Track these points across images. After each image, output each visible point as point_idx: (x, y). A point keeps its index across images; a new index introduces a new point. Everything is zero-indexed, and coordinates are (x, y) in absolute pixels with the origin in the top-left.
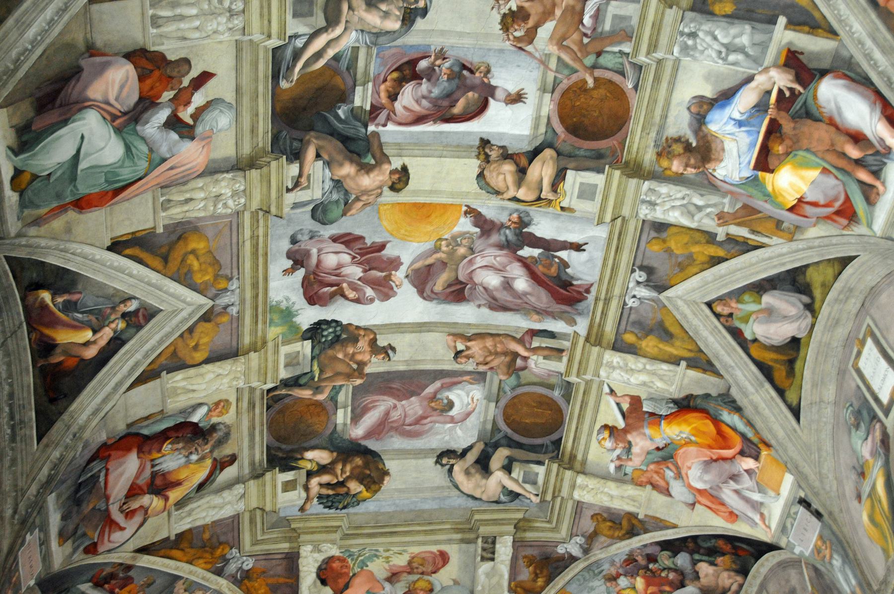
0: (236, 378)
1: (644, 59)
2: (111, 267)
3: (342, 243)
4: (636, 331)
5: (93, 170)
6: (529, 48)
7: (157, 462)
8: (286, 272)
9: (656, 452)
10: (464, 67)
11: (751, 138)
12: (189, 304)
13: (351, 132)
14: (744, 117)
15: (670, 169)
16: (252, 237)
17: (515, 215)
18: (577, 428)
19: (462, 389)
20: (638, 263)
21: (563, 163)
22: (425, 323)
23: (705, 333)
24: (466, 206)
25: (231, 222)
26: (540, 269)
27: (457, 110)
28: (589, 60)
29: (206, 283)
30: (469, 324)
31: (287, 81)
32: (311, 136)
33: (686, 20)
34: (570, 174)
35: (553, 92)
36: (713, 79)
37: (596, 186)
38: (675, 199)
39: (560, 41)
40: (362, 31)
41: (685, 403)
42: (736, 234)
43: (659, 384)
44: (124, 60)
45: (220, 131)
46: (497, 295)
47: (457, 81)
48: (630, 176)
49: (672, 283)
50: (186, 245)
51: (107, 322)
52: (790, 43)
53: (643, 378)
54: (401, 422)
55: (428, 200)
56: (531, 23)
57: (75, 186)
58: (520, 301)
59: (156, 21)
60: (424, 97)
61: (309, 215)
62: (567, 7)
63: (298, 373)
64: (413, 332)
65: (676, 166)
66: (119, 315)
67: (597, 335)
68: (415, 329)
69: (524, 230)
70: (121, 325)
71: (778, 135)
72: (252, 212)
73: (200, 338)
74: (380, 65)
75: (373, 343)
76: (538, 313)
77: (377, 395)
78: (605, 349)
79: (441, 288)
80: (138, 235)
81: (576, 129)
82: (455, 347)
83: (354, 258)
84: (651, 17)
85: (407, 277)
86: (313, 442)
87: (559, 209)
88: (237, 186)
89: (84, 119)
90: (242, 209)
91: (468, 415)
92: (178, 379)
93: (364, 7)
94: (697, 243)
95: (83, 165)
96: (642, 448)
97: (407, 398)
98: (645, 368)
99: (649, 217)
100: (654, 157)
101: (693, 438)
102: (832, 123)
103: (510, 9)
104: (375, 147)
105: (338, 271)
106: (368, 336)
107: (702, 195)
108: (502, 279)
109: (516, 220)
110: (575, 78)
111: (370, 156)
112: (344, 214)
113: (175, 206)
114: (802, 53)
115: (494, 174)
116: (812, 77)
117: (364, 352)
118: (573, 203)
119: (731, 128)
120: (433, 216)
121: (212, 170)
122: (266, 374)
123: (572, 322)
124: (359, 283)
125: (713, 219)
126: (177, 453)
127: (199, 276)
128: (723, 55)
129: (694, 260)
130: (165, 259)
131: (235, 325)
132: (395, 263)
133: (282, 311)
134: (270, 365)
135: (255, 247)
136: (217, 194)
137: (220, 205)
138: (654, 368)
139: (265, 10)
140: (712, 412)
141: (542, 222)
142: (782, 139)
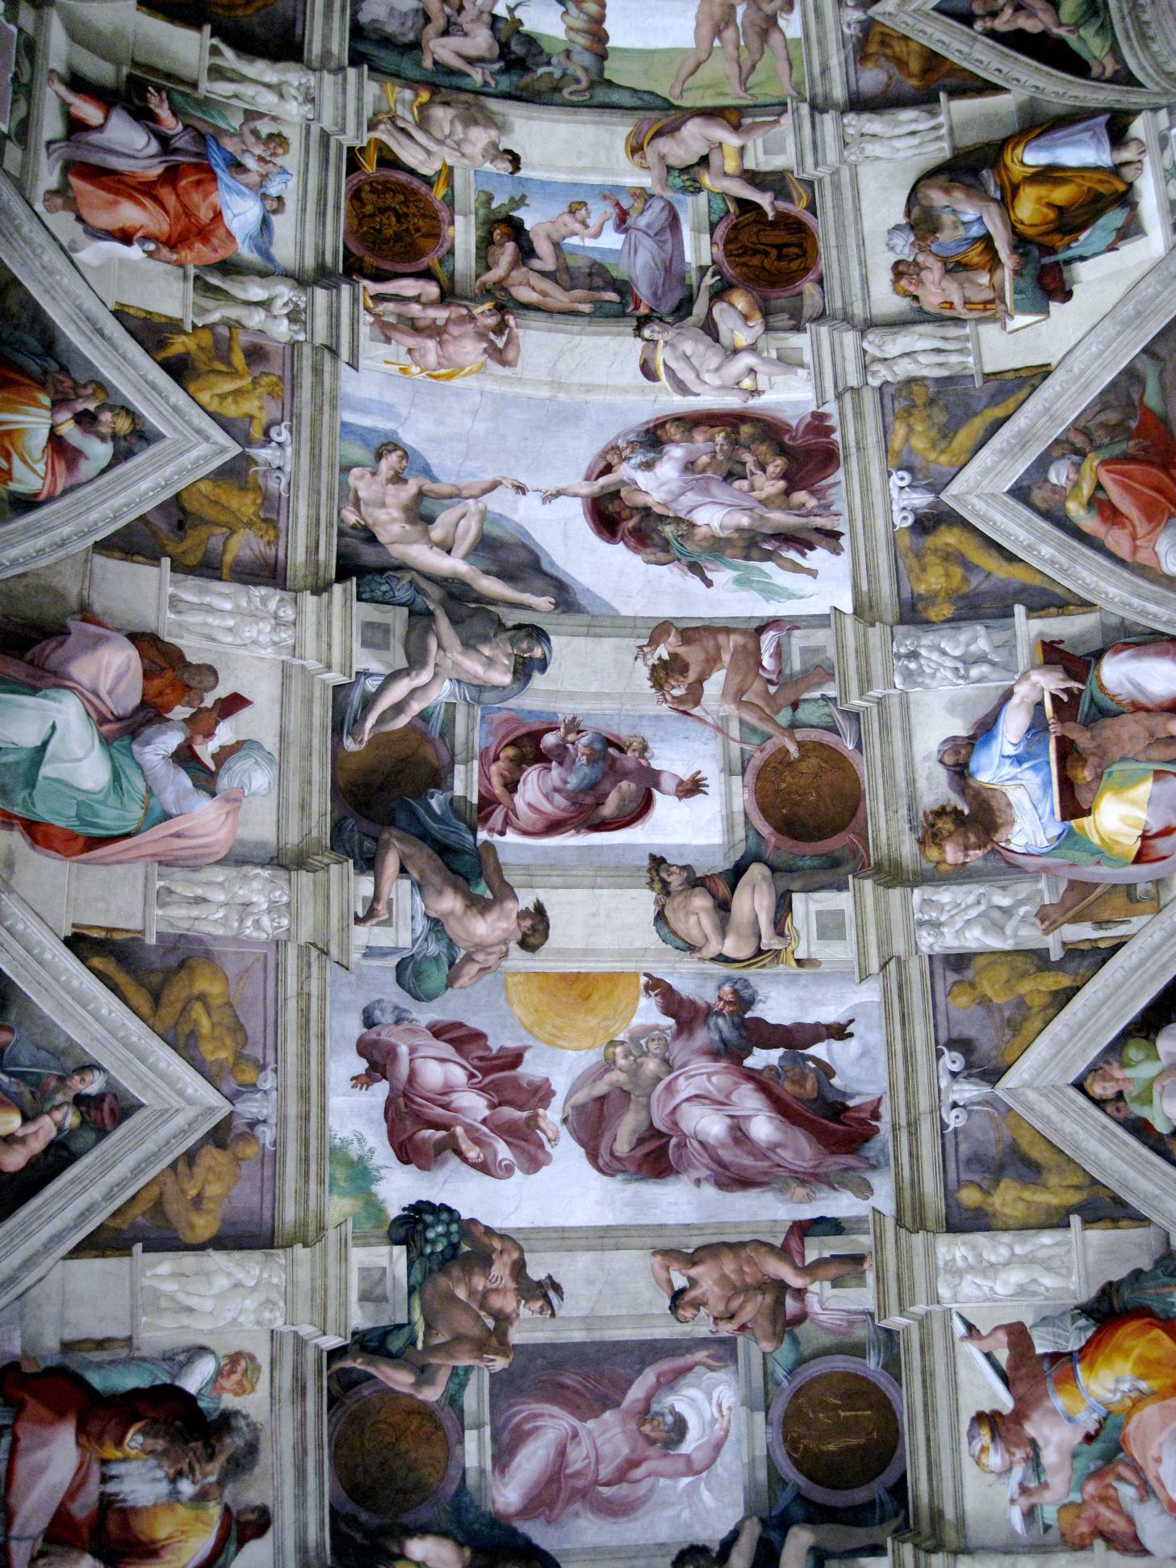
0: (268, 1303)
1: (858, 702)
2: (67, 987)
3: (446, 1041)
4: (976, 1178)
5: (62, 788)
6: (696, 711)
7: (115, 1469)
8: (357, 1081)
9: (1086, 1447)
10: (609, 743)
11: (1042, 774)
12: (190, 1101)
13: (452, 840)
14: (1021, 749)
15: (944, 861)
16: (299, 995)
17: (727, 988)
18: (928, 1439)
19: (698, 1386)
20: (943, 1036)
21: (785, 882)
22: (608, 1228)
23: (1092, 1145)
24: (646, 975)
25: (266, 955)
26: (787, 1088)
27: (609, 809)
28: (784, 717)
29: (220, 1063)
30: (687, 1226)
31: (355, 740)
32: (390, 835)
33: (898, 637)
34: (798, 899)
35: (743, 774)
36: (960, 709)
37: (842, 912)
38: (968, 907)
39: (738, 697)
40: (459, 681)
41: (1104, 1306)
42: (1075, 938)
43: (1048, 1281)
44: (126, 641)
45: (253, 794)
46: (726, 1155)
47: (601, 764)
48: (889, 885)
49: (1009, 1059)
50: (192, 982)
51: (48, 1106)
52: (1041, 634)
53: (1016, 1277)
54: (591, 1476)
56: (692, 676)
57: (30, 795)
58: (766, 1164)
59: (175, 603)
60: (556, 790)
61: (391, 976)
62: (735, 648)
64: (589, 1249)
65: (952, 854)
66: (70, 1098)
67: (914, 1209)
68: (592, 1242)
69: (748, 1015)
70: (72, 1119)
71: (1075, 755)
72: (299, 947)
73: (206, 1182)
74: (490, 733)
75: (519, 1268)
76: (803, 1182)
77: (539, 1400)
78: (935, 1233)
80: (117, 936)
81: (791, 827)
82: (670, 1282)
83: (472, 1076)
84: (850, 642)
85: (565, 1121)
86: (423, 1514)
87: (794, 964)
88: (277, 893)
89: (60, 702)
90: (284, 937)
91: (718, 1447)
92: (160, 1273)
93: (459, 648)
94: (1024, 975)
95: (46, 770)
96: (1059, 1449)
97: (596, 1415)
98: (1013, 1254)
99: (937, 949)
100: (916, 847)
101: (1143, 1385)
102: (1137, 707)
103: (660, 659)
104: (490, 869)
105: (446, 1098)
107: (1004, 888)
108: (728, 1121)
109: (729, 997)
110: (770, 747)
112: (450, 984)
113: (178, 904)
114: (1061, 642)
115: (681, 915)
116: (1088, 666)
117: (505, 1291)
118: (813, 949)
119: (1008, 770)
120: (595, 997)
121: (239, 858)
122: (325, 1307)
123: (865, 1190)
124: (484, 1129)
125: (1033, 924)
126: (152, 1462)
127: (210, 1047)
128: (962, 672)
129: (1030, 1008)
130: (156, 998)
131: (268, 1172)
132: (541, 1093)
133: (351, 1164)
136: (246, 901)
137: (249, 923)
138: (1029, 1247)
139: (324, 629)
140: (1156, 1307)
141: (773, 994)
142: (1082, 760)
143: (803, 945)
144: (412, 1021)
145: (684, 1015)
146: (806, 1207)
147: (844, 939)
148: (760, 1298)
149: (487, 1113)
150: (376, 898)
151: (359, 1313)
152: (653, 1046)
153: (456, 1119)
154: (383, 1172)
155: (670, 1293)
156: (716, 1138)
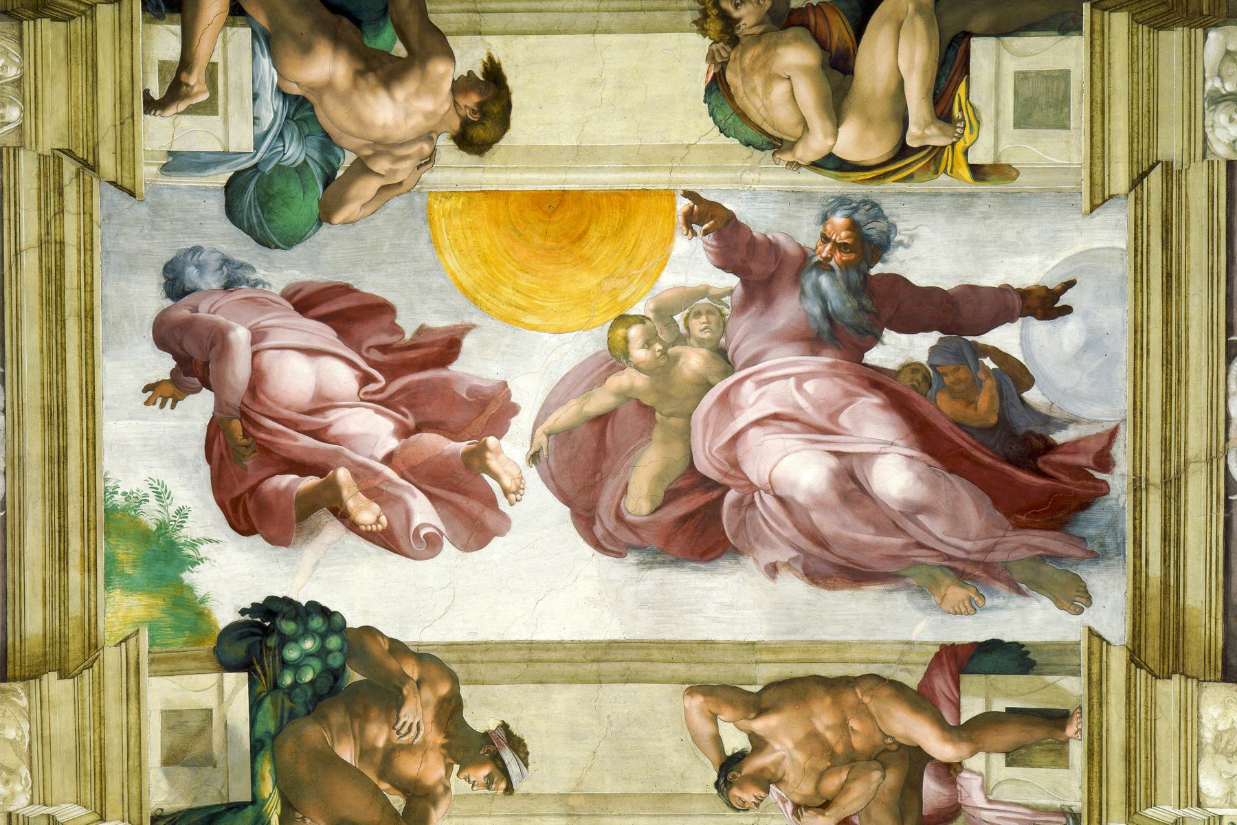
3: (323, 318)
16: (43, 243)
17: (839, 220)
22: (611, 645)
24: (688, 194)
34: (982, 50)
37: (1065, 75)
46: (827, 524)
48: (1159, 24)
55: (575, 181)
58: (897, 541)
61: (216, 205)
63: (209, 799)
69: (874, 271)
72: (42, 158)
75: (450, 709)
76: (962, 577)
79: (645, 507)
82: (717, 740)
83: (366, 379)
85: (534, 458)
87: (966, 174)
90: (12, 141)
106: (433, 686)
108: (832, 462)
109: (843, 236)
111: (389, 32)
112: (325, 215)
115: (758, 81)
117: (424, 747)
118: (1005, 145)
120: (594, 234)
122: (102, 776)
124: (389, 472)
133: (144, 536)
134: (114, 738)
135: (54, 277)
141: (924, 232)
143: (986, 136)
144: (256, 283)
145: (756, 267)
146: (967, 620)
147: (1066, 127)
148: (876, 775)
149: (393, 444)
150: (186, 63)
151: (164, 785)
152: (697, 325)
153: (338, 454)
154: (203, 550)
155: (717, 759)
156: (810, 493)
